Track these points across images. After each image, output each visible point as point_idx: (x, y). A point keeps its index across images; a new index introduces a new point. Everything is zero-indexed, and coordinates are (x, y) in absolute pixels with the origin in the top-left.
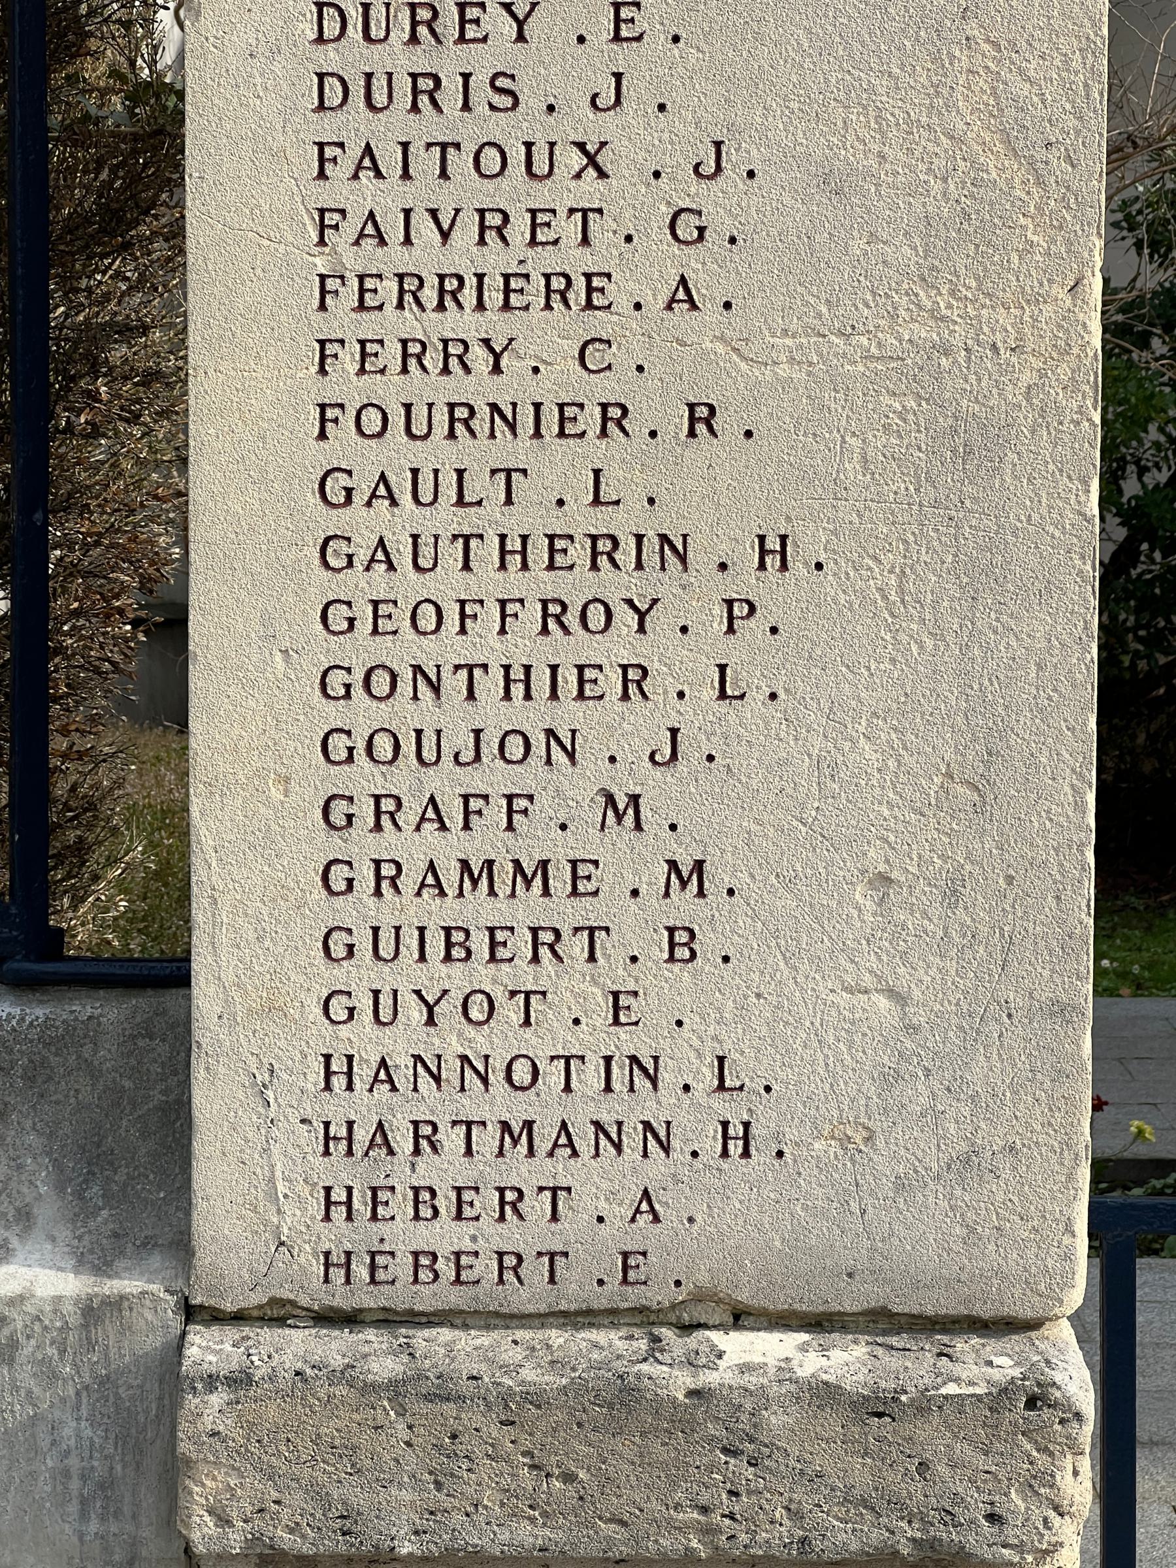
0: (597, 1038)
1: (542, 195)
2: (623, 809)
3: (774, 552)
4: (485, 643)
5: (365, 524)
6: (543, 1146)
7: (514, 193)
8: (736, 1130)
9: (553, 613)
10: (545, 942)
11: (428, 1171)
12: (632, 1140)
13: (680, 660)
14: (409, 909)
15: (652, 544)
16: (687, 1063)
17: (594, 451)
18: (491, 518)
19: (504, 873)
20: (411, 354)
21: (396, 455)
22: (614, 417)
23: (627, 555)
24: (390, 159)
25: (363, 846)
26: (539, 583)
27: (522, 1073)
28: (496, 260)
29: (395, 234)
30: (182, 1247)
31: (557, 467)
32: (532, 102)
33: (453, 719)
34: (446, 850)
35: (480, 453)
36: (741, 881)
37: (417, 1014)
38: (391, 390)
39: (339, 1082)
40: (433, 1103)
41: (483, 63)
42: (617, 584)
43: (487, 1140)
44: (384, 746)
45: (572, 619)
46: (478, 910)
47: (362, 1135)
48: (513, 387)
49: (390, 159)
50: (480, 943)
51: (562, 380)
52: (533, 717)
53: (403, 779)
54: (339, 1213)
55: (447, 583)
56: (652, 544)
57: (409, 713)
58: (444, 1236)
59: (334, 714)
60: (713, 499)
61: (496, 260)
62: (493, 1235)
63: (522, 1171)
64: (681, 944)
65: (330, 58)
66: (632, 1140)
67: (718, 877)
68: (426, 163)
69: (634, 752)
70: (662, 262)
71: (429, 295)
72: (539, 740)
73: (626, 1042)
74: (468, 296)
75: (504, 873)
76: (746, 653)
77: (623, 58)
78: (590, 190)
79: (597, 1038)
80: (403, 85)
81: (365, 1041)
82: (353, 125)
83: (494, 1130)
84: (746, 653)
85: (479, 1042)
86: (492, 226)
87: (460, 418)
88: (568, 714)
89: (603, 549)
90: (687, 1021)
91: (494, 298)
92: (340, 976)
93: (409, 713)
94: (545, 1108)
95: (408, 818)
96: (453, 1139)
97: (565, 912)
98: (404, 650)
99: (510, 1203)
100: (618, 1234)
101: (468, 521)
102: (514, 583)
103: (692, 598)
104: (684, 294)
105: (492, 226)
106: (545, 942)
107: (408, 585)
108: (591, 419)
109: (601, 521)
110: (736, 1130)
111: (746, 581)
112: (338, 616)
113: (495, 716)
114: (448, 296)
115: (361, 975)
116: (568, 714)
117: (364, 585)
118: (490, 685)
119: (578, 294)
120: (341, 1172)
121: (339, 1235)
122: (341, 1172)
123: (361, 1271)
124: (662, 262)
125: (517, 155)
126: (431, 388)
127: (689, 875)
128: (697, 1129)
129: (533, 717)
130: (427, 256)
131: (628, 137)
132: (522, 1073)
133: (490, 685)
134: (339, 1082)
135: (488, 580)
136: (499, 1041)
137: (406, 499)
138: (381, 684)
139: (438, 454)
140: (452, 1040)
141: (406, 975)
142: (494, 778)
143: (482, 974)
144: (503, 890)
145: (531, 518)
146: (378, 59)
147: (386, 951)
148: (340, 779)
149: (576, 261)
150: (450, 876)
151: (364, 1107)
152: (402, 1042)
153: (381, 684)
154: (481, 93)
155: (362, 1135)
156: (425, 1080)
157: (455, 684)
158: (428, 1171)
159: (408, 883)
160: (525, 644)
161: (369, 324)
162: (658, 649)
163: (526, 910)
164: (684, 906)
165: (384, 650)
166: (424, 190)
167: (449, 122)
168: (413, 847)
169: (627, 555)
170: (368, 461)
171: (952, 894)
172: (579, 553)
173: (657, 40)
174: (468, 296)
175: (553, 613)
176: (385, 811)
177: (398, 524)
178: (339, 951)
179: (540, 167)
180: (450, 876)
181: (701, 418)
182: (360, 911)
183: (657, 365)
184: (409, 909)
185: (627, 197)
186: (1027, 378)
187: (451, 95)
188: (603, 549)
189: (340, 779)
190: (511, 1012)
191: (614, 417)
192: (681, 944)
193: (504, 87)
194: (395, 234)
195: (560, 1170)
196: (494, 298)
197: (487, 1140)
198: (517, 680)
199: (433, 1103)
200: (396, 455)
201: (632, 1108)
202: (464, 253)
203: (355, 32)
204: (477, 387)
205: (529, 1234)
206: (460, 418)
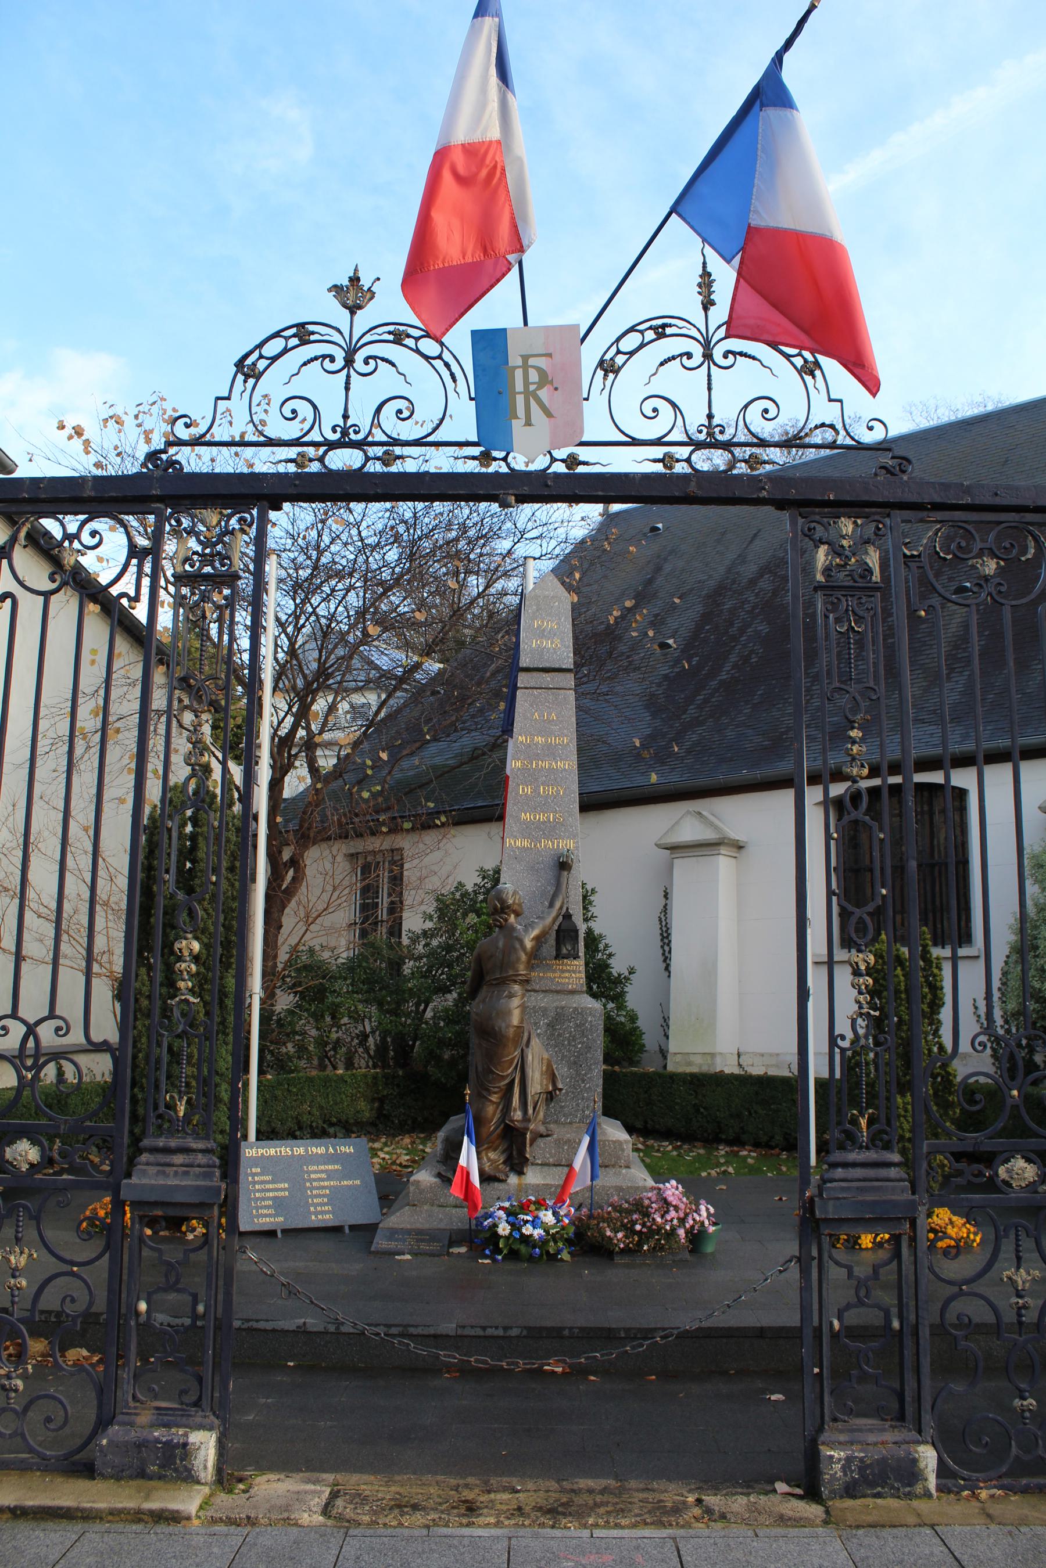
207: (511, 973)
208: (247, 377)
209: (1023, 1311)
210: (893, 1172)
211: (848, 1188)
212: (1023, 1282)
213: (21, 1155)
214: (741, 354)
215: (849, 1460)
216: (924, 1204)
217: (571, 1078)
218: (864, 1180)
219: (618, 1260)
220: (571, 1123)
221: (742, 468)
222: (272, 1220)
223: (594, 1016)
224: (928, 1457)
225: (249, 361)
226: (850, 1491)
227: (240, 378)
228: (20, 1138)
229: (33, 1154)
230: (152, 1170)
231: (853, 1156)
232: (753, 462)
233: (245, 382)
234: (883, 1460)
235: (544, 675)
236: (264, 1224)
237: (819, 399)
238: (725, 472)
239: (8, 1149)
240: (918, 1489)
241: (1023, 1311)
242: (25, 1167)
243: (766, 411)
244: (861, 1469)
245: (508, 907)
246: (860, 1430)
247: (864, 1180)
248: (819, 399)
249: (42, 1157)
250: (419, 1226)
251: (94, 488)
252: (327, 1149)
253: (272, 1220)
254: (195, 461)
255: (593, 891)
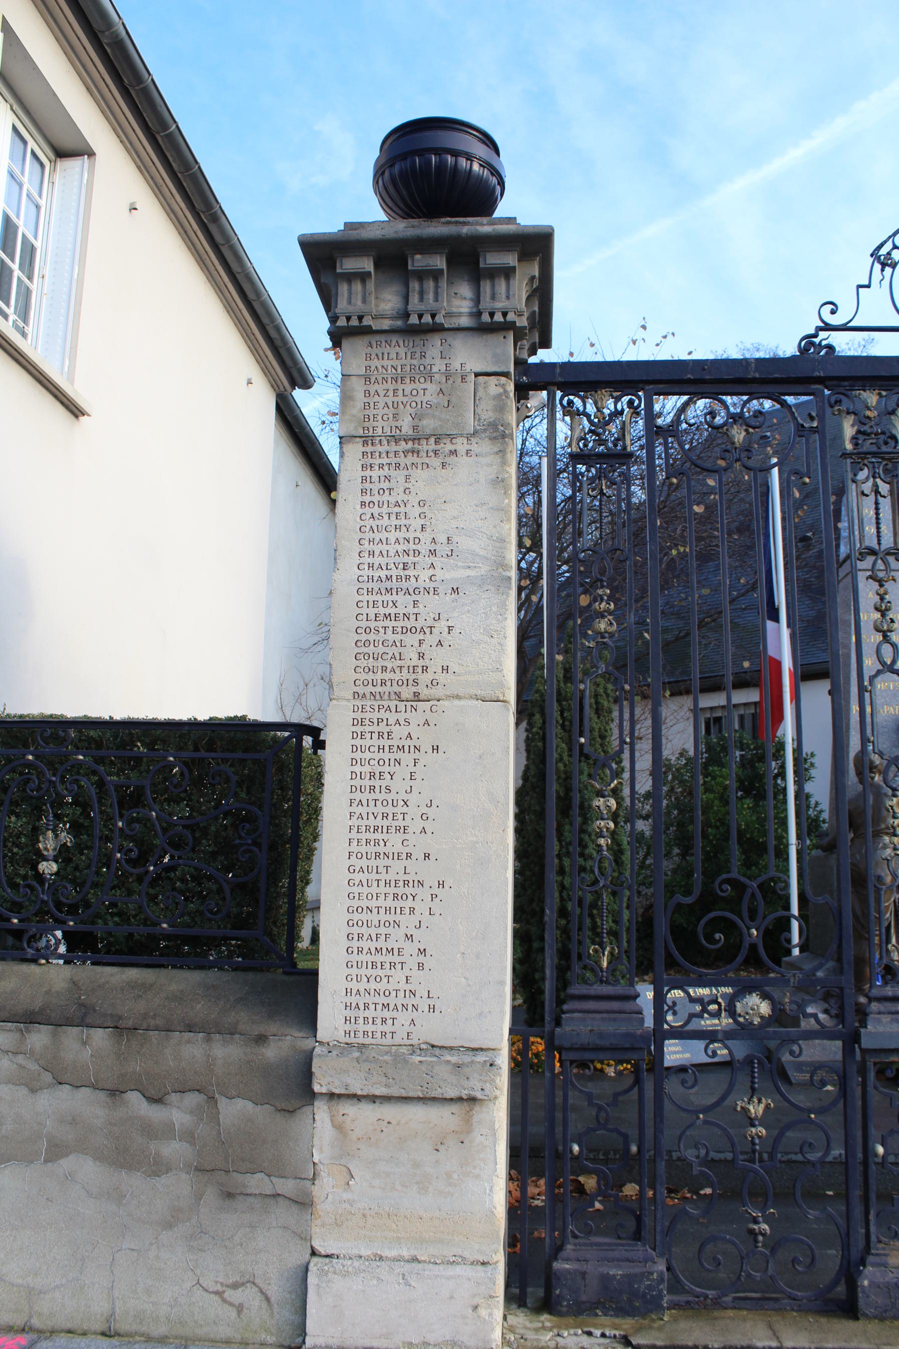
0: (403, 986)
1: (395, 810)
2: (409, 937)
3: (441, 884)
4: (381, 902)
5: (357, 877)
6: (391, 1009)
7: (389, 810)
8: (432, 1006)
9: (395, 896)
10: (392, 965)
11: (367, 1013)
12: (410, 1008)
13: (421, 908)
14: (363, 957)
15: (416, 882)
16: (422, 992)
17: (405, 863)
18: (383, 876)
19: (384, 950)
20: (368, 842)
21: (364, 863)
22: (409, 856)
23: (411, 884)
24: (365, 802)
25: (355, 944)
26: (393, 890)
27: (387, 993)
28: (385, 823)
29: (365, 817)
30: (315, 1037)
31: (397, 866)
32: (394, 791)
33: (374, 918)
34: (373, 945)
35: (381, 863)
36: (433, 953)
37: (366, 980)
38: (363, 849)
39: (349, 994)
40: (368, 999)
41: (384, 784)
42: (409, 890)
43: (379, 1007)
44: (360, 923)
45: (399, 897)
46: (378, 958)
47: (353, 1005)
48: (388, 849)
49: (365, 802)
50: (379, 965)
51: (398, 848)
52: (391, 918)
53: (364, 930)
54: (348, 1022)
55: (374, 890)
56: (416, 882)
57: (365, 916)
58: (370, 1028)
59: (350, 916)
60: (429, 873)
61: (385, 823)
62: (379, 1028)
63: (387, 1014)
64: (421, 966)
65: (353, 783)
66: (410, 1008)
67: (428, 953)
68: (372, 803)
69: (411, 926)
70: (419, 824)
71: (372, 830)
72: (392, 923)
73: (408, 987)
74: (380, 830)
75: (384, 950)
76: (436, 906)
77: (412, 783)
78: (405, 809)
79: (403, 986)
80: (368, 788)
81: (354, 986)
82: (358, 796)
83: (381, 1005)
84: (436, 906)
85: (378, 986)
86: (385, 816)
87: (377, 855)
88: (398, 918)
89: (406, 883)
90: (421, 982)
91: (385, 830)
92: (350, 971)
93: (365, 916)
94: (392, 1001)
95: (365, 938)
96: (372, 1007)
97: (396, 959)
98: (364, 903)
99: (384, 1021)
100: (407, 1028)
101: (378, 877)
102: (387, 889)
103: (424, 893)
104: (424, 830)
105: (385, 816)
106: (392, 965)
107: (365, 890)
108: (404, 856)
109: (406, 877)
110: (432, 1006)
111: (436, 890)
112: (351, 896)
113: (383, 917)
114: (376, 830)
115: (354, 971)
116: (398, 918)
117: (356, 890)
118: (382, 911)
119: (402, 830)
120: (348, 1013)
121: (348, 1027)
122: (348, 1013)
123: (352, 1034)
124: (419, 824)
125: (390, 802)
126: (371, 849)
127: (422, 952)
128: (423, 1006)
129: (391, 918)
130: (372, 822)
131: (413, 799)
132: (387, 993)
133: (382, 911)
134: (349, 994)
135: (382, 889)
136: (382, 986)
137: (366, 871)
138: (360, 910)
139: (373, 863)
140: (373, 985)
141: (363, 971)
142: (383, 930)
143: (379, 972)
144: (384, 953)
145: (391, 876)
146: (363, 783)
147: (359, 966)
148: (351, 930)
149: (402, 824)
150: (373, 951)
151: (354, 1000)
152: (362, 986)
153: (360, 910)
154: (383, 789)
155: (353, 1005)
156: (367, 994)
157: (375, 911)
158: (367, 1013)
159: (364, 952)
160: (389, 902)
161: (359, 836)
162: (417, 905)
163: (390, 958)
164: (421, 958)
165: (360, 903)
166: (372, 808)
167: (377, 795)
168: (365, 944)
169: (411, 884)
170: (358, 864)
171: (478, 957)
172: (401, 884)
173: (419, 780)
174: (380, 830)
175: (395, 896)
176: (360, 937)
177: (364, 877)
178: (349, 966)
179: (395, 804)
180: (373, 951)
181: (427, 856)
182: (355, 958)
183: (418, 844)
184: (363, 957)
185: (412, 811)
186: (494, 849)
187: (377, 790)
188: (406, 883)
189: (351, 930)
190: (385, 980)
191: (409, 856)
192: (421, 966)
193: (388, 789)
194: (365, 817)
195: (394, 1014)
196: (385, 830)
197: (379, 1007)
198: (388, 910)
199: (368, 999)
200: (364, 863)
201: (410, 1001)
202: (379, 822)
203: (359, 777)
204: (381, 849)
205: (387, 1028)
206: (377, 855)
207: (883, 826)
208: (884, 265)
213: (752, 1009)
222: (681, 1056)
225: (883, 251)
227: (878, 267)
228: (750, 993)
229: (765, 1008)
230: (886, 1019)
233: (882, 270)
236: (676, 1060)
239: (738, 1004)
242: (756, 1021)
245: (876, 767)
249: (773, 1010)
250: (817, 1058)
251: (756, 370)
252: (711, 991)
253: (681, 1056)
254: (846, 344)
255: (812, 755)
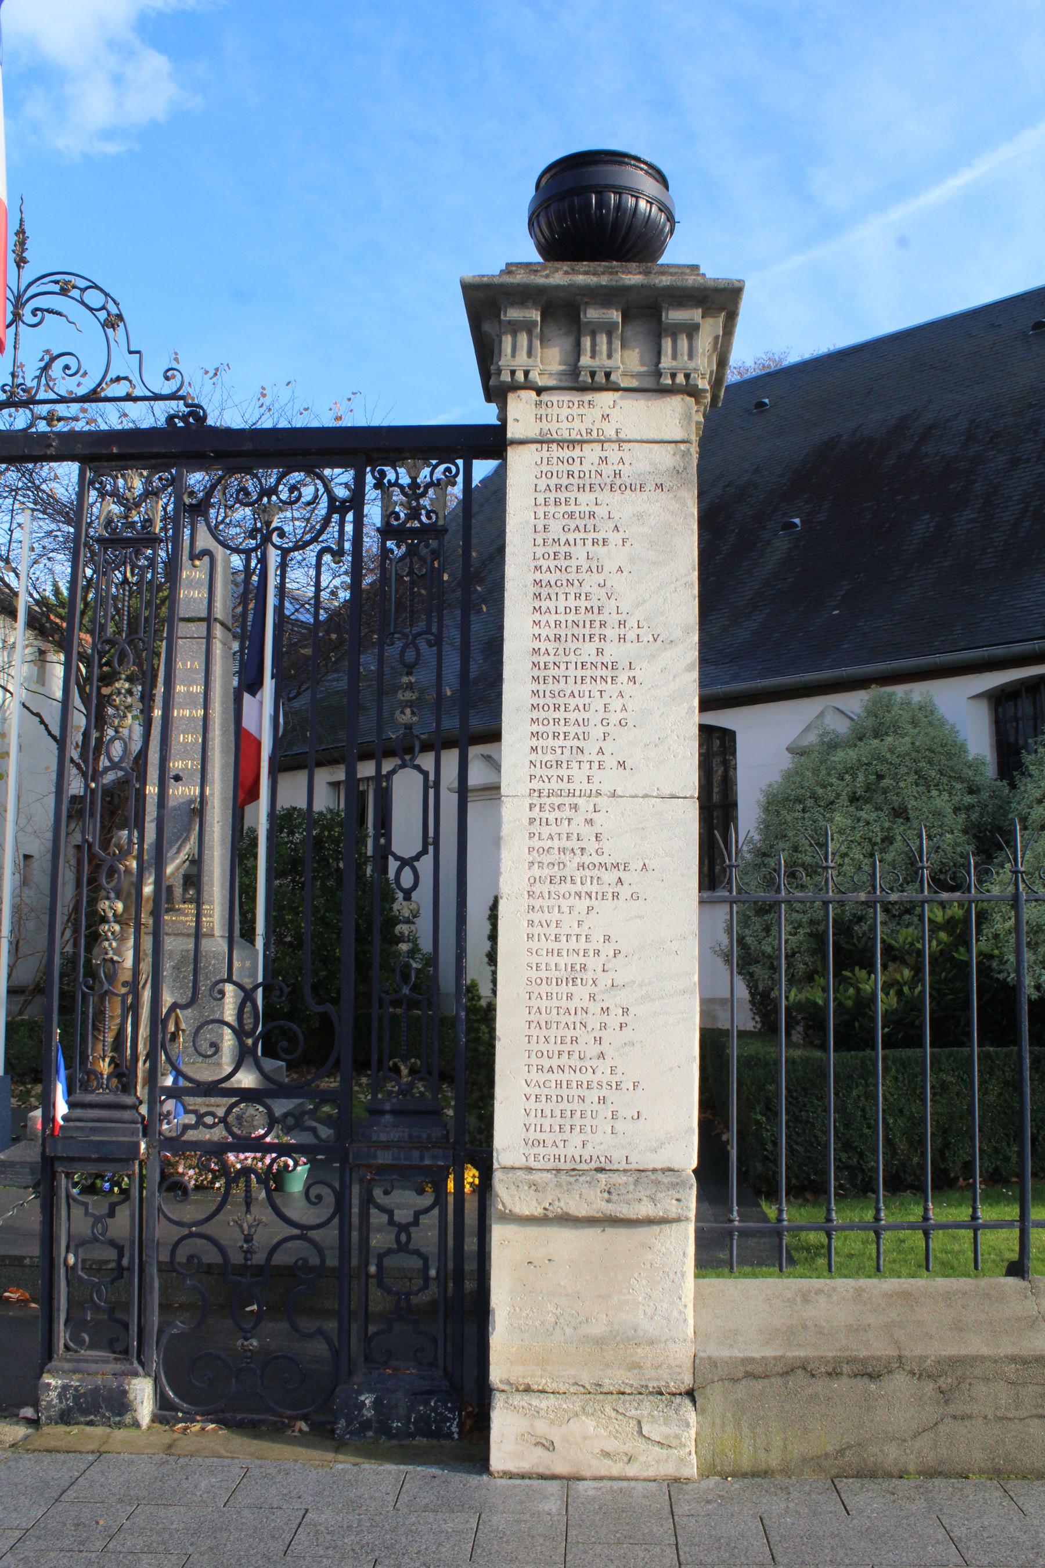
209: (249, 1256)
210: (127, 1115)
211: (82, 1128)
212: (249, 1227)
214: (50, 311)
215: (65, 1388)
216: (155, 1147)
217: (195, 1019)
218: (99, 1120)
219: (194, 1197)
220: (193, 1063)
221: (42, 427)
223: (218, 959)
224: (143, 1394)
226: (65, 1418)
231: (90, 1098)
232: (50, 419)
234: (95, 1391)
235: (190, 625)
237: (119, 352)
238: (25, 430)
240: (128, 1419)
241: (249, 1256)
243: (67, 367)
244: (76, 1398)
246: (86, 1361)
247: (99, 1120)
248: (119, 352)
